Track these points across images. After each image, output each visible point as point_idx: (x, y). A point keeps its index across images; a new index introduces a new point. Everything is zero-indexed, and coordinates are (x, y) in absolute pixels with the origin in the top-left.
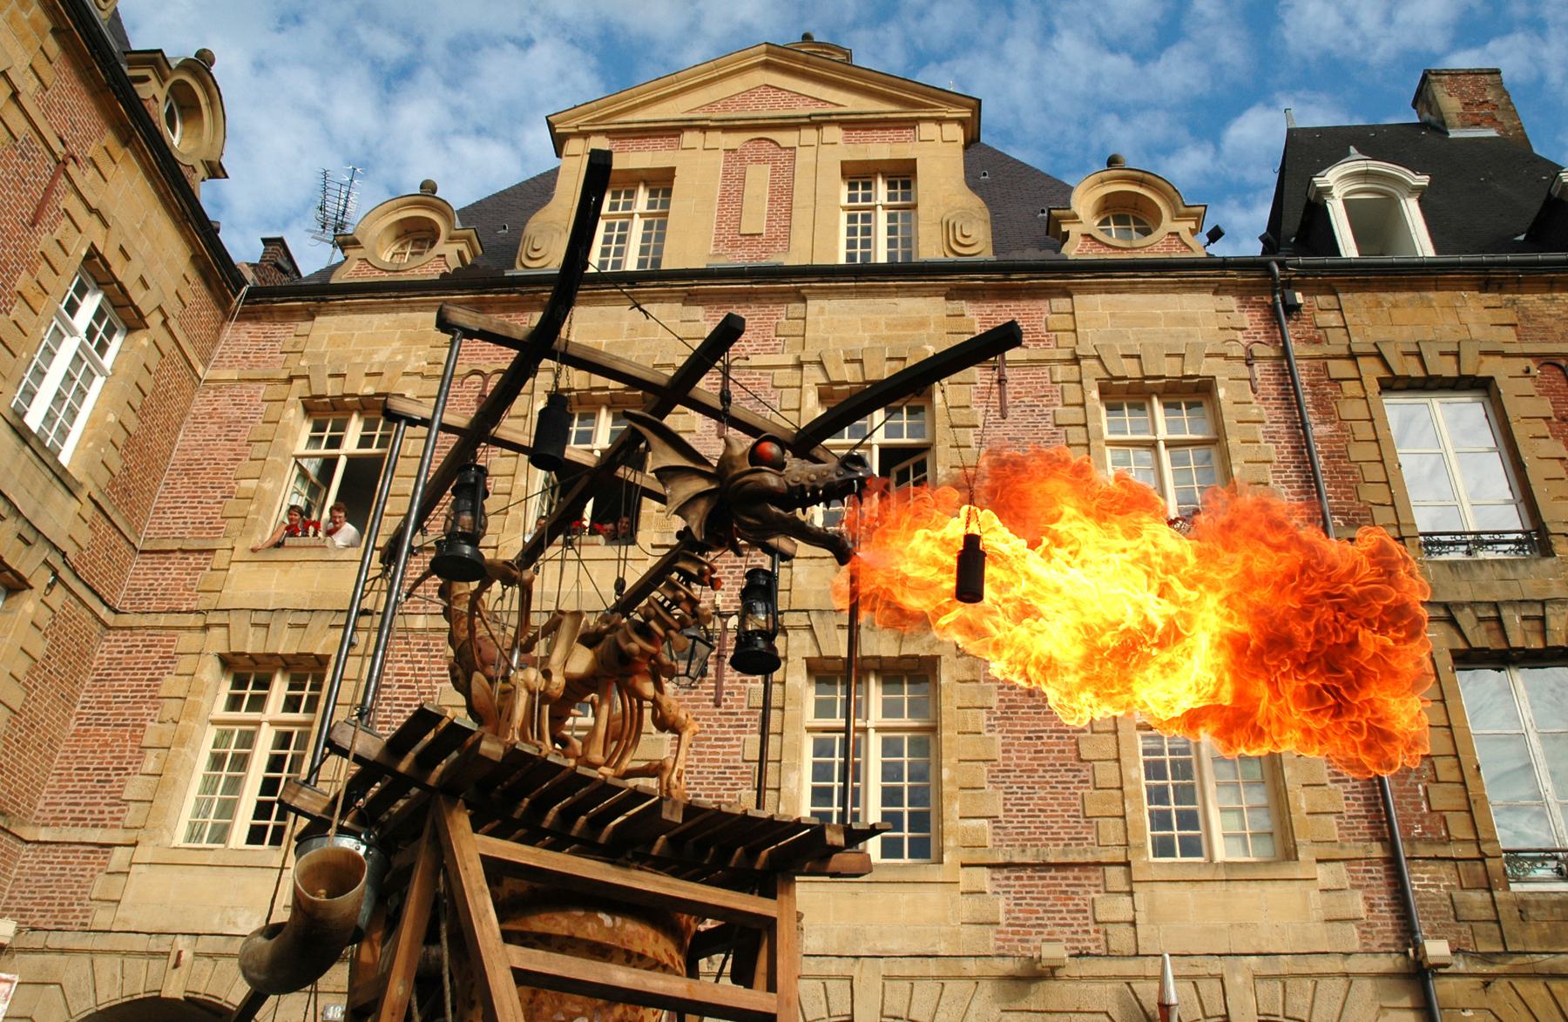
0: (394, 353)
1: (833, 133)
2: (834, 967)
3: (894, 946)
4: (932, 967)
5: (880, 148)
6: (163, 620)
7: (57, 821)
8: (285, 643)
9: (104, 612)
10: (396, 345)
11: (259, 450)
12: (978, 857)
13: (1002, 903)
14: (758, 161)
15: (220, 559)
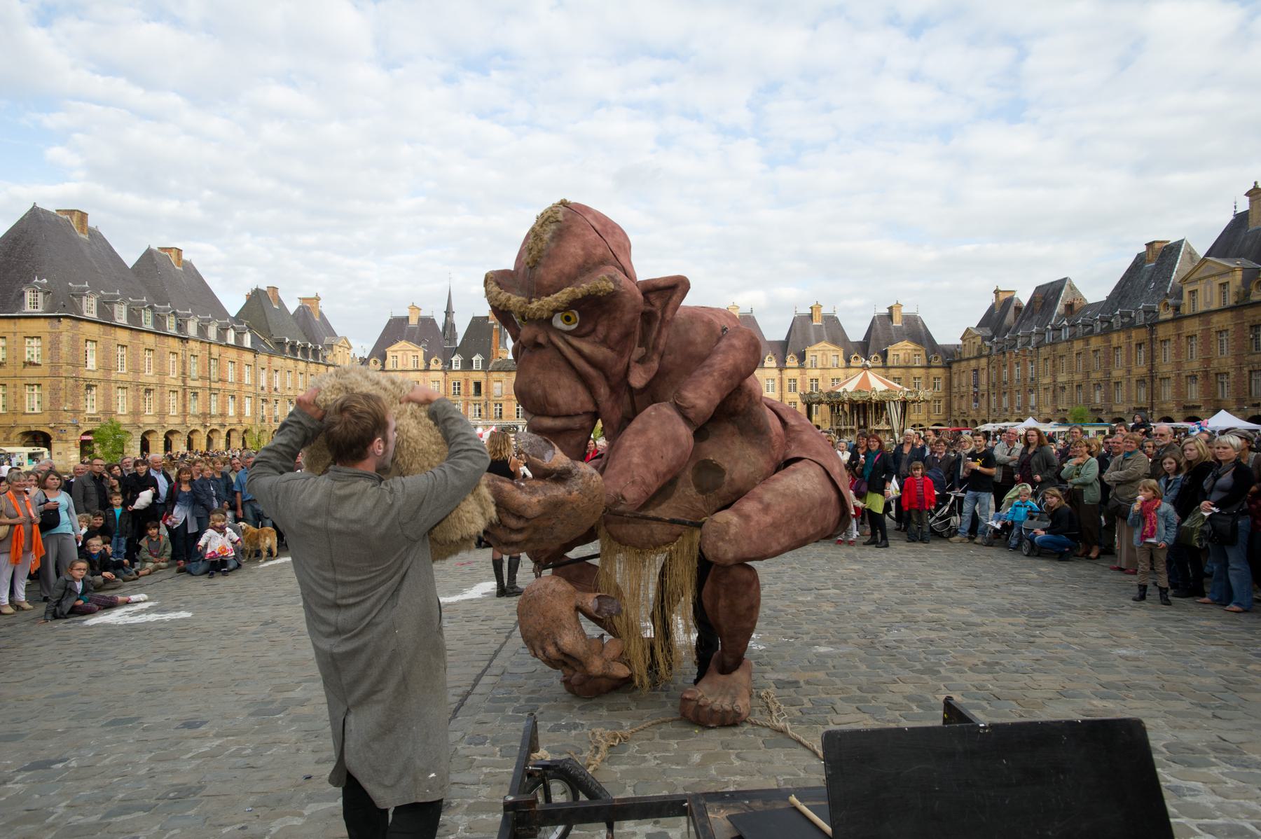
5: (415, 354)
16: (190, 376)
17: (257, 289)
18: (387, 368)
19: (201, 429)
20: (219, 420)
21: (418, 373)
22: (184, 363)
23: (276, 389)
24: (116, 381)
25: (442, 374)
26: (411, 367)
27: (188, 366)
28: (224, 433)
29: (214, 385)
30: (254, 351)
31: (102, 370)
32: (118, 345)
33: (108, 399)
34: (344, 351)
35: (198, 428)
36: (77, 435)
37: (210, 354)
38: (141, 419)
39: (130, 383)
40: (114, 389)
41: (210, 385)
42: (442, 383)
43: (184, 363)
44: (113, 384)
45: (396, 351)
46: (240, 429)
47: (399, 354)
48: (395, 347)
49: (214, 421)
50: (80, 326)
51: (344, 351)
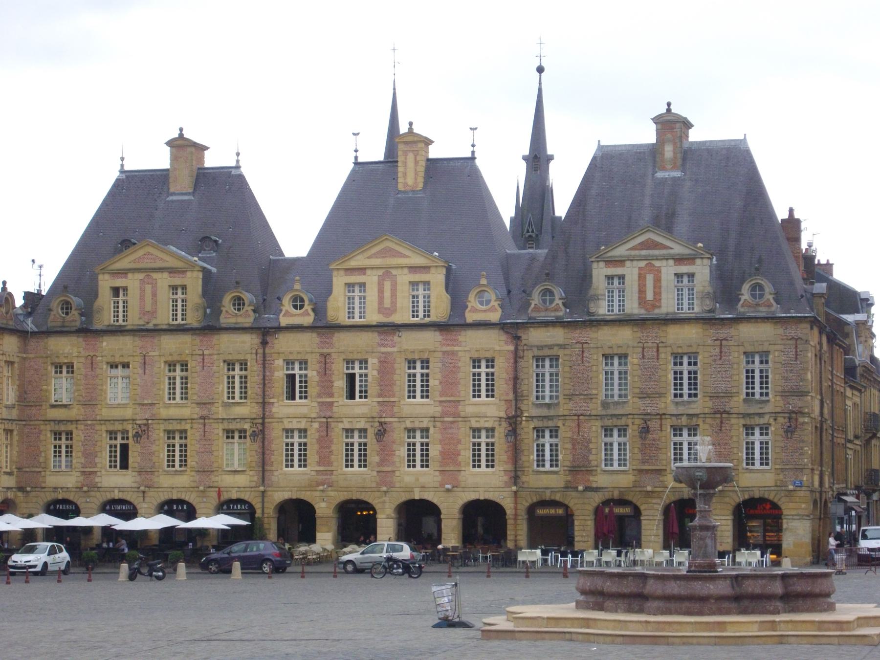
0: (69, 350)
1: (166, 275)
2: (169, 490)
3: (179, 486)
4: (185, 489)
5: (177, 281)
6: (36, 423)
7: (29, 467)
8: (63, 428)
9: (24, 423)
10: (69, 347)
11: (44, 378)
12: (194, 469)
13: (198, 477)
14: (148, 284)
15: (44, 407)
18: (97, 326)
21: (187, 338)
25: (246, 343)
26: (164, 318)
42: (254, 368)
45: (124, 273)
47: (132, 282)
48: (125, 262)
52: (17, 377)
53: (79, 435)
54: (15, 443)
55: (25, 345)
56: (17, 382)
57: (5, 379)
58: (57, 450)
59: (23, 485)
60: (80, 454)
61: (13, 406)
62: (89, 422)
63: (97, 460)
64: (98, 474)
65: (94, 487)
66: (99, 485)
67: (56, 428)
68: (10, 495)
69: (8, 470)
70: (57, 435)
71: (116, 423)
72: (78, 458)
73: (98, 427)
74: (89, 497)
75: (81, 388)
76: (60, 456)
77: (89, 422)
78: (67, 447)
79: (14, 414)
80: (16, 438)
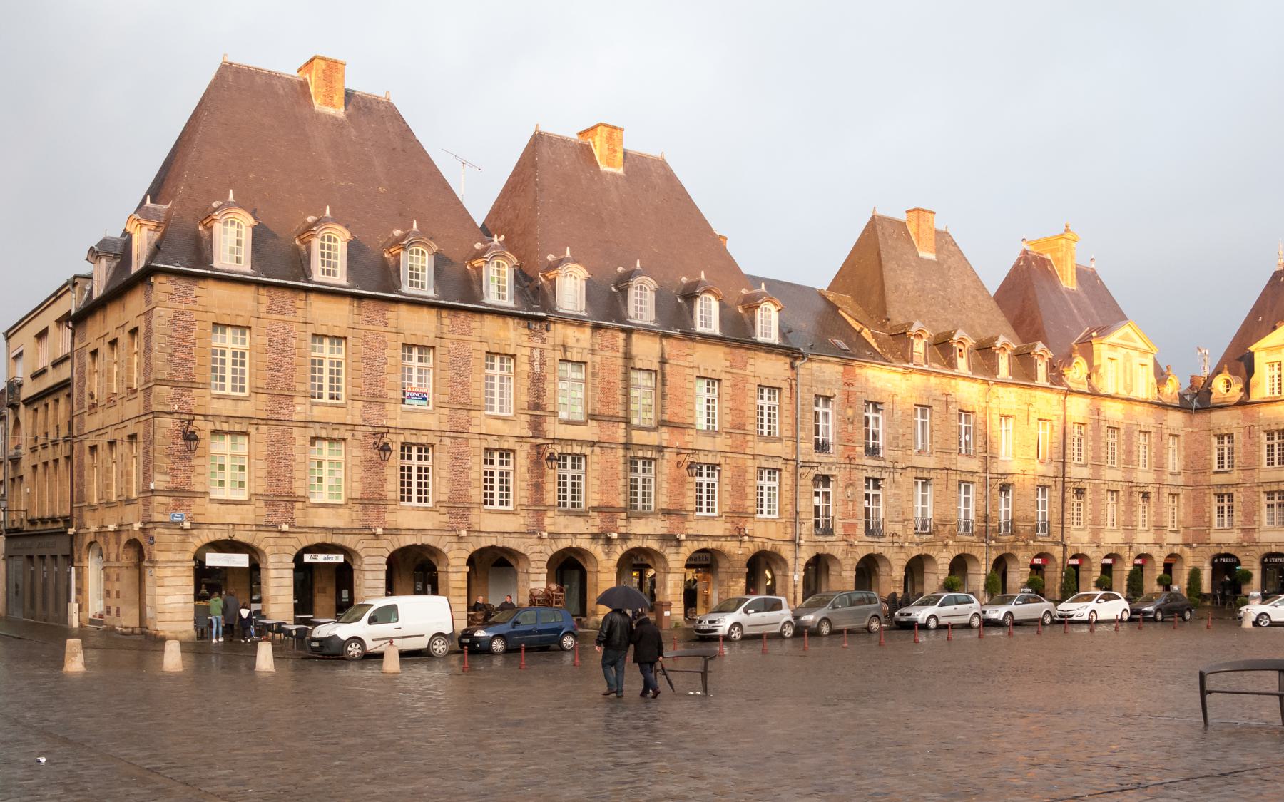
8: (1224, 491)
16: (555, 414)
17: (873, 217)
19: (597, 550)
20: (658, 526)
22: (537, 381)
23: (873, 451)
24: (306, 424)
27: (549, 387)
28: (676, 559)
29: (638, 437)
30: (789, 351)
31: (264, 397)
32: (408, 347)
33: (280, 465)
34: (1127, 358)
35: (583, 543)
36: (183, 550)
37: (628, 357)
38: (388, 516)
39: (353, 427)
40: (300, 441)
41: (628, 435)
43: (537, 381)
44: (296, 431)
46: (739, 551)
49: (639, 527)
50: (197, 291)
51: (1127, 358)
52: (1183, 449)
53: (1239, 497)
54: (1182, 505)
55: (1191, 421)
56: (1183, 453)
57: (1171, 450)
58: (1221, 513)
59: (1190, 541)
60: (1240, 513)
61: (1179, 474)
62: (1248, 485)
63: (1256, 518)
64: (1257, 530)
65: (1255, 543)
66: (1257, 540)
67: (1219, 491)
68: (1176, 550)
69: (1175, 529)
70: (1220, 497)
71: (1272, 484)
72: (1238, 517)
73: (1256, 489)
74: (1248, 551)
75: (1241, 455)
76: (1223, 516)
77: (1248, 485)
78: (1229, 508)
79: (1180, 480)
80: (1182, 501)
